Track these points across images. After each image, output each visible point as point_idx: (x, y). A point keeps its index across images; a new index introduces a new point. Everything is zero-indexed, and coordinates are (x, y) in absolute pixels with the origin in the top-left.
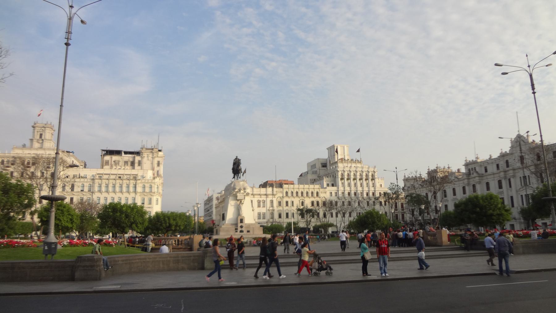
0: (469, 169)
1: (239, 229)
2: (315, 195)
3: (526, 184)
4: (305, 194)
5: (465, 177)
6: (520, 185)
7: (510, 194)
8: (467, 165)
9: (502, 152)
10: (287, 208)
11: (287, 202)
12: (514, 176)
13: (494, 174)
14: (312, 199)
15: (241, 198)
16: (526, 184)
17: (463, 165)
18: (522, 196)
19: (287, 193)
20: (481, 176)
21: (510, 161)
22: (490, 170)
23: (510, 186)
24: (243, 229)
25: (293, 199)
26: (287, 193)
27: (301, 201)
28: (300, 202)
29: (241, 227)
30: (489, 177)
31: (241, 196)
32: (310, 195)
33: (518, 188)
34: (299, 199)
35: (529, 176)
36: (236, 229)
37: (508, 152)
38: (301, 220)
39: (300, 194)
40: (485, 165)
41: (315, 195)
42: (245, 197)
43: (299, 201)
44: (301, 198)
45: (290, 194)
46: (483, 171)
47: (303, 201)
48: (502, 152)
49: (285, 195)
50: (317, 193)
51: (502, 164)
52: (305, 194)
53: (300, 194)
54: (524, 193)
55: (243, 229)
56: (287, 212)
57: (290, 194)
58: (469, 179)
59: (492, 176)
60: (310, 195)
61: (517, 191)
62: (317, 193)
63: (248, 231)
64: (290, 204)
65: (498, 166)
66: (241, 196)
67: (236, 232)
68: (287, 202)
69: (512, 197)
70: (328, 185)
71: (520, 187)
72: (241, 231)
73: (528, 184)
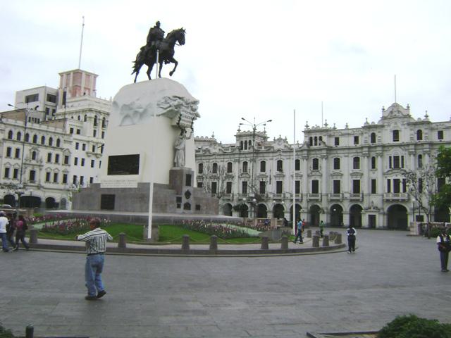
0: (311, 138)
1: (184, 200)
2: (54, 143)
3: (397, 166)
4: (39, 141)
5: (305, 147)
6: (388, 167)
7: (373, 177)
8: (307, 132)
9: (367, 123)
10: (8, 160)
11: (9, 150)
13: (349, 149)
14: (50, 150)
15: (186, 123)
16: (397, 166)
18: (389, 181)
19: (10, 133)
20: (329, 149)
21: (415, 136)
22: (344, 142)
23: (374, 166)
24: (192, 201)
25: (19, 146)
26: (10, 133)
27: (32, 151)
29: (188, 194)
30: (339, 152)
32: (47, 142)
33: (386, 171)
34: (31, 148)
35: (402, 157)
36: (179, 200)
37: (376, 124)
38: (30, 184)
39: (31, 139)
40: (335, 134)
41: (54, 143)
42: (192, 123)
44: (33, 146)
45: (15, 137)
46: (332, 143)
47: (37, 152)
48: (367, 123)
49: (7, 137)
50: (58, 141)
51: (364, 140)
52: (39, 141)
53: (31, 139)
54: (392, 178)
55: (192, 201)
56: (8, 166)
57: (15, 137)
58: (309, 151)
59: (347, 151)
60: (47, 142)
61: (384, 174)
62: (58, 141)
63: (198, 207)
64: (13, 153)
65: (356, 140)
66: (186, 119)
67: (179, 206)
68: (9, 150)
69: (374, 182)
70: (72, 131)
71: (388, 169)
72: (187, 206)
73: (400, 166)
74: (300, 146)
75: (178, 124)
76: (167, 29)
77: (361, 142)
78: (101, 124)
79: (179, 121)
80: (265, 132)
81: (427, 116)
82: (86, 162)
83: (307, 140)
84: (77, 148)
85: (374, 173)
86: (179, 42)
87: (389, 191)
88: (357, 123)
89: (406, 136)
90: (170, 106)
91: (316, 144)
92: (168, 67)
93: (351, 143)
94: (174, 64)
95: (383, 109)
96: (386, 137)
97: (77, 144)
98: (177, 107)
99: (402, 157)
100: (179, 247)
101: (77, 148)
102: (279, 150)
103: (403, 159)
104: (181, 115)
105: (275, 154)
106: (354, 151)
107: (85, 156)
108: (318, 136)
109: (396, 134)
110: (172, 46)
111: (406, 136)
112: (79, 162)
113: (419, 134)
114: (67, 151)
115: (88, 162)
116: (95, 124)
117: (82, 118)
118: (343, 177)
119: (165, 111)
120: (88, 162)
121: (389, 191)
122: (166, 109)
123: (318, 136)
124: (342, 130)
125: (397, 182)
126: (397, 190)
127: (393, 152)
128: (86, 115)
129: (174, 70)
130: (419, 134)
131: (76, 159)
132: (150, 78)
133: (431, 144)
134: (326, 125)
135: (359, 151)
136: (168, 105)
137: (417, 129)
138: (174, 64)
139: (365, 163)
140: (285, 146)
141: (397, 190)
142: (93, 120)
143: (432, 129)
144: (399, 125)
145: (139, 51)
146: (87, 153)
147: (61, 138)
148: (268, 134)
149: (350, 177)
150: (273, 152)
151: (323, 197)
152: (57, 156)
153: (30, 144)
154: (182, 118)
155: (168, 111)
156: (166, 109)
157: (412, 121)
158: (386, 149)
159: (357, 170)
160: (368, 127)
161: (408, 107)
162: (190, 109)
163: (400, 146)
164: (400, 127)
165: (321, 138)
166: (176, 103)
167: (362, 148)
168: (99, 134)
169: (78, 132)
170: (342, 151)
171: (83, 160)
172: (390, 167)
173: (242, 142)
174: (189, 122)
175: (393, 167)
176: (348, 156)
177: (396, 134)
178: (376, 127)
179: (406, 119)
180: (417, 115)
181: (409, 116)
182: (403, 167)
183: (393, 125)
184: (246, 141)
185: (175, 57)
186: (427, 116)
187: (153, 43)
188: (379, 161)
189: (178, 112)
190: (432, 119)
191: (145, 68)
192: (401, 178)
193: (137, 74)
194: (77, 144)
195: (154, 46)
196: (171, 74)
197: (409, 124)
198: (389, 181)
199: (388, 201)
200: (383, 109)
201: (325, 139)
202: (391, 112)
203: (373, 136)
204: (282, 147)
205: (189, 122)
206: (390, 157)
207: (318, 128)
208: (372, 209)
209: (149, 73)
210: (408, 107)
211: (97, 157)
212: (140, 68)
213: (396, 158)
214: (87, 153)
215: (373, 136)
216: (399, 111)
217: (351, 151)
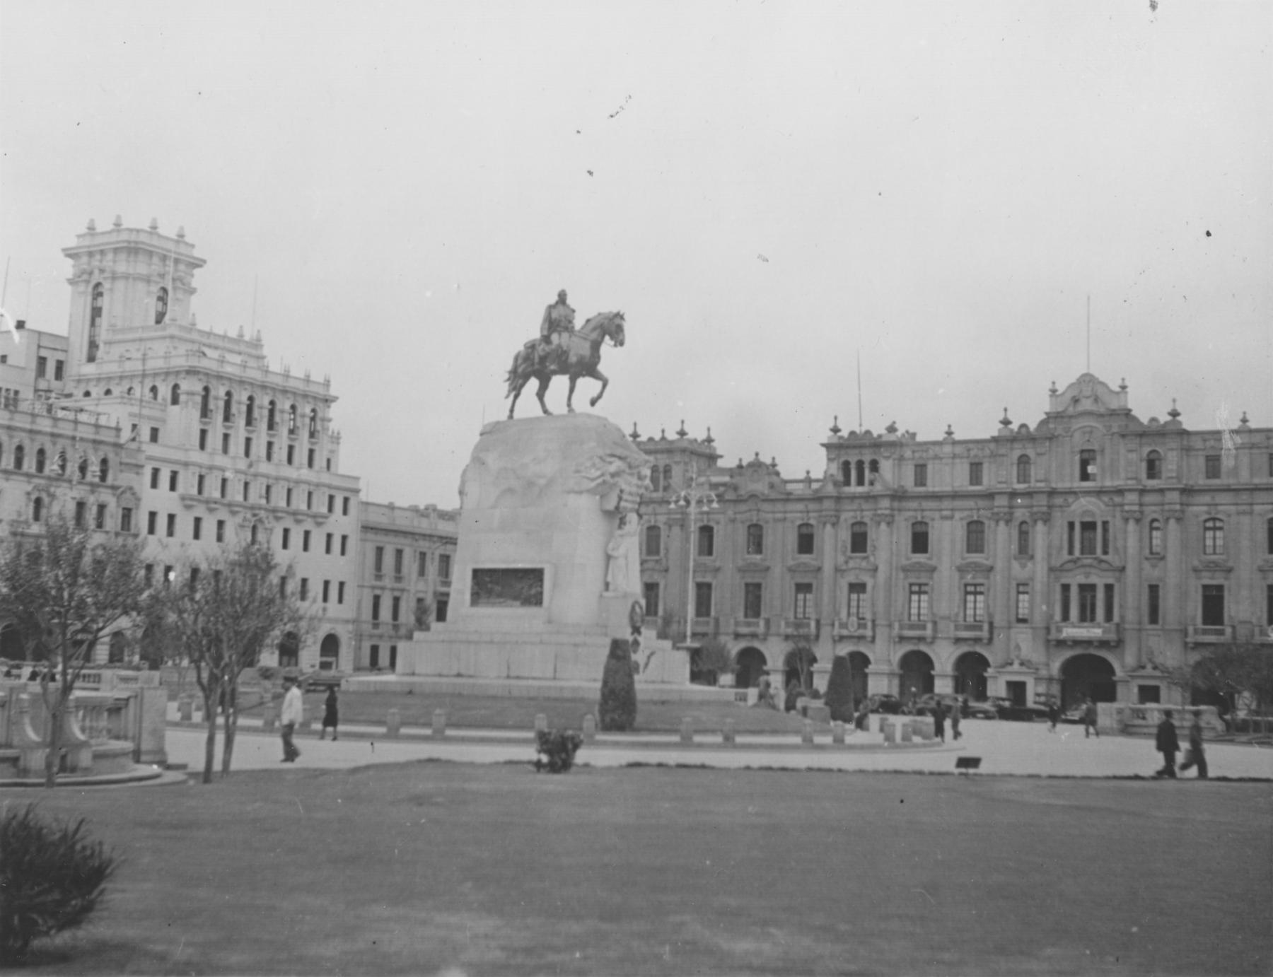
12: (1047, 519)
13: (955, 496)
14: (79, 492)
16: (1088, 548)
17: (823, 445)
18: (1066, 588)
20: (899, 496)
27: (34, 497)
28: (29, 499)
31: (630, 498)
34: (29, 488)
35: (1105, 523)
43: (28, 494)
44: (36, 481)
46: (909, 482)
52: (52, 466)
53: (29, 464)
61: (1051, 569)
65: (976, 471)
71: (1066, 557)
73: (1099, 550)
74: (815, 486)
75: (617, 508)
76: (584, 311)
77: (989, 480)
78: (265, 420)
79: (619, 503)
80: (709, 440)
81: (1174, 414)
82: (178, 522)
83: (835, 469)
84: (154, 484)
85: (1023, 566)
86: (612, 338)
90: (603, 475)
91: (860, 482)
92: (587, 386)
93: (958, 478)
94: (599, 384)
95: (1054, 391)
97: (156, 472)
98: (613, 475)
99: (1105, 523)
101: (154, 484)
102: (753, 496)
103: (1105, 530)
104: (622, 491)
105: (743, 507)
106: (970, 503)
107: (176, 509)
108: (867, 458)
110: (596, 346)
112: (162, 523)
114: (128, 495)
115: (184, 525)
116: (205, 412)
117: (165, 391)
118: (935, 575)
119: (593, 484)
120: (184, 525)
122: (593, 480)
123: (867, 458)
124: (935, 443)
128: (176, 387)
129: (600, 396)
131: (153, 515)
132: (545, 411)
133: (1187, 491)
136: (598, 473)
137: (1146, 450)
138: (599, 384)
139: (1001, 539)
140: (772, 486)
142: (199, 399)
143: (1187, 450)
145: (521, 348)
146: (183, 498)
147: (111, 456)
148: (719, 447)
149: (956, 575)
150: (736, 502)
151: (878, 631)
152: (102, 508)
153: (28, 475)
154: (625, 496)
155: (599, 485)
156: (593, 480)
158: (1058, 501)
159: (975, 558)
161: (1124, 387)
162: (636, 477)
163: (1099, 493)
165: (874, 466)
166: (613, 468)
167: (990, 496)
168: (215, 440)
169: (154, 435)
171: (171, 518)
172: (1071, 552)
174: (633, 502)
176: (952, 518)
182: (1105, 552)
185: (601, 368)
186: (1174, 414)
187: (555, 338)
188: (1039, 534)
189: (615, 485)
190: (1188, 423)
191: (533, 384)
192: (1099, 580)
193: (516, 397)
194: (156, 472)
195: (559, 346)
196: (593, 403)
198: (1066, 588)
199: (1061, 643)
200: (1054, 391)
202: (1076, 401)
204: (761, 487)
205: (633, 502)
208: (1016, 667)
209: (541, 395)
210: (1124, 387)
211: (234, 513)
212: (522, 386)
213: (1089, 527)
214: (183, 498)
217: (958, 503)
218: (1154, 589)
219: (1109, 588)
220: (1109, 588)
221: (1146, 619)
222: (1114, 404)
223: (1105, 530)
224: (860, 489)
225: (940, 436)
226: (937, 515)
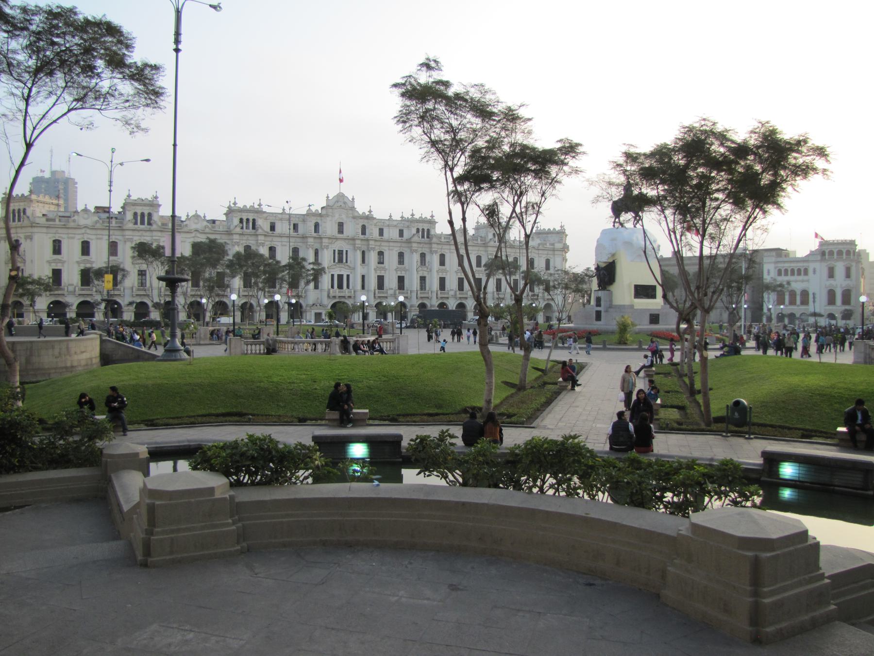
3: (340, 260)
16: (340, 260)
18: (333, 276)
30: (275, 239)
35: (347, 251)
46: (267, 228)
54: (336, 273)
65: (295, 227)
87: (332, 287)
88: (299, 208)
89: (351, 229)
91: (247, 228)
95: (328, 197)
96: (329, 228)
99: (347, 251)
100: (601, 346)
103: (347, 254)
109: (341, 225)
111: (351, 229)
113: (364, 228)
121: (332, 287)
125: (340, 277)
126: (340, 286)
127: (338, 245)
130: (364, 228)
134: (235, 204)
135: (298, 240)
141: (340, 286)
144: (344, 216)
151: (126, 291)
157: (356, 214)
160: (310, 214)
161: (353, 199)
164: (344, 218)
170: (279, 239)
172: (334, 261)
173: (135, 214)
175: (337, 261)
177: (341, 225)
178: (320, 215)
179: (351, 212)
180: (361, 208)
181: (353, 208)
182: (347, 262)
183: (337, 216)
184: (143, 215)
186: (370, 211)
197: (354, 218)
200: (328, 197)
201: (260, 222)
203: (317, 226)
206: (334, 251)
207: (245, 208)
210: (353, 199)
213: (341, 252)
215: (317, 226)
216: (345, 203)
218: (363, 277)
219: (348, 276)
220: (348, 276)
221: (330, 287)
222: (350, 205)
223: (347, 254)
224: (142, 227)
225: (281, 211)
226: (94, 237)
